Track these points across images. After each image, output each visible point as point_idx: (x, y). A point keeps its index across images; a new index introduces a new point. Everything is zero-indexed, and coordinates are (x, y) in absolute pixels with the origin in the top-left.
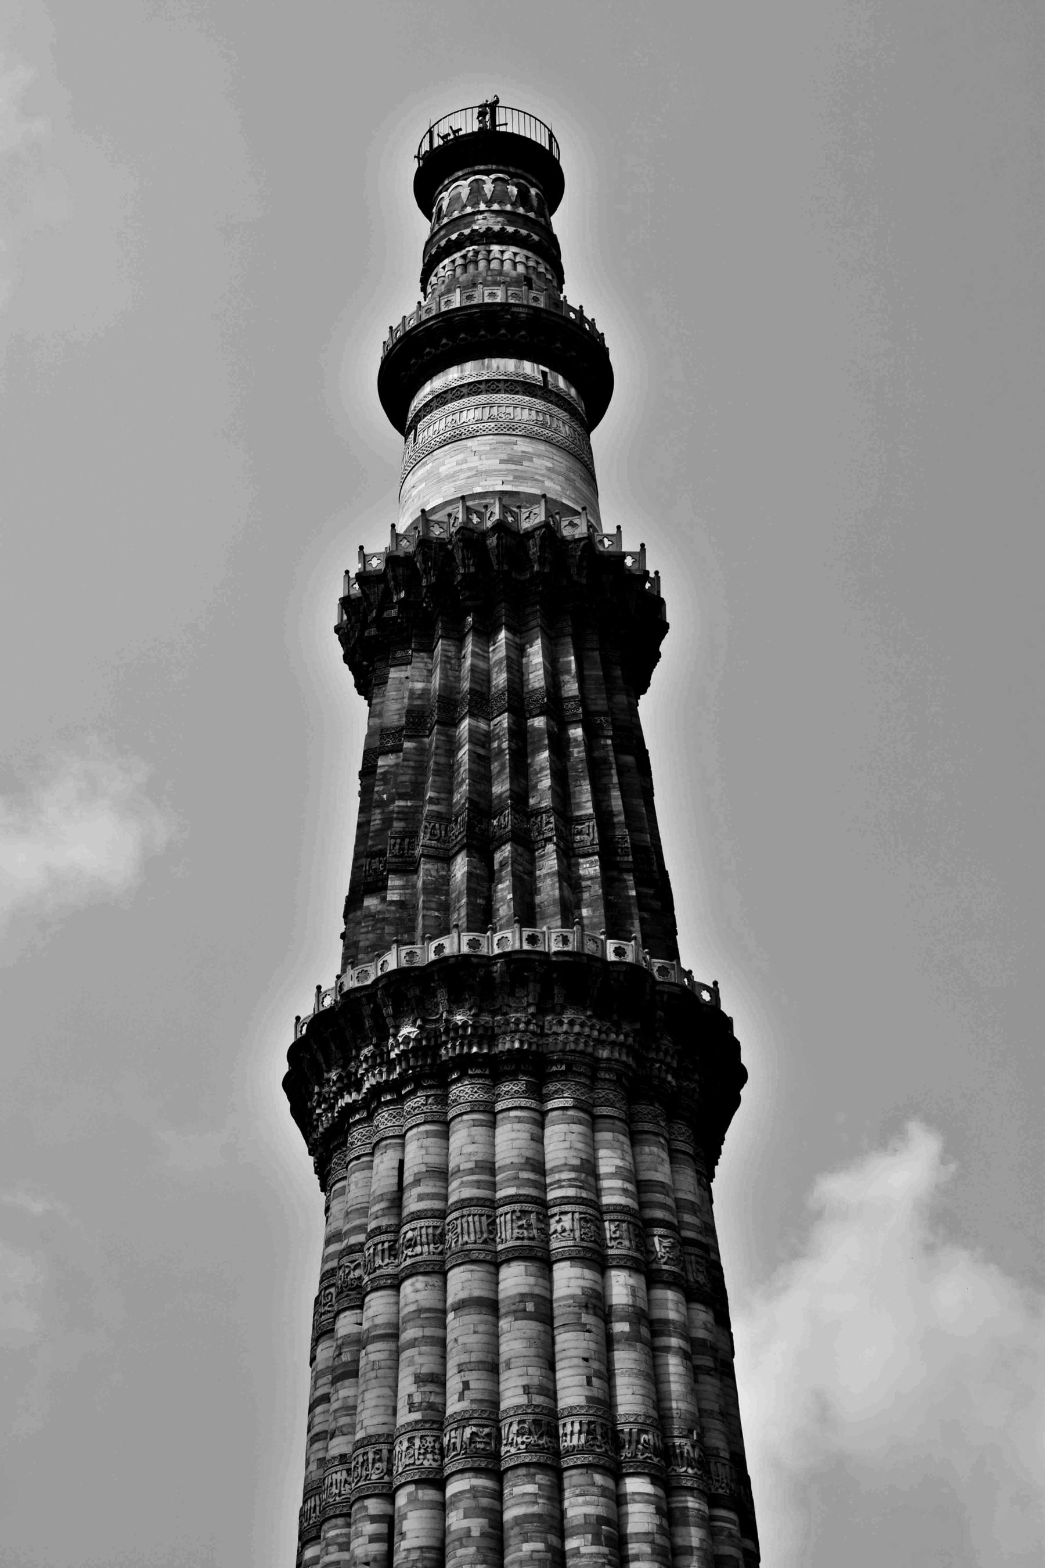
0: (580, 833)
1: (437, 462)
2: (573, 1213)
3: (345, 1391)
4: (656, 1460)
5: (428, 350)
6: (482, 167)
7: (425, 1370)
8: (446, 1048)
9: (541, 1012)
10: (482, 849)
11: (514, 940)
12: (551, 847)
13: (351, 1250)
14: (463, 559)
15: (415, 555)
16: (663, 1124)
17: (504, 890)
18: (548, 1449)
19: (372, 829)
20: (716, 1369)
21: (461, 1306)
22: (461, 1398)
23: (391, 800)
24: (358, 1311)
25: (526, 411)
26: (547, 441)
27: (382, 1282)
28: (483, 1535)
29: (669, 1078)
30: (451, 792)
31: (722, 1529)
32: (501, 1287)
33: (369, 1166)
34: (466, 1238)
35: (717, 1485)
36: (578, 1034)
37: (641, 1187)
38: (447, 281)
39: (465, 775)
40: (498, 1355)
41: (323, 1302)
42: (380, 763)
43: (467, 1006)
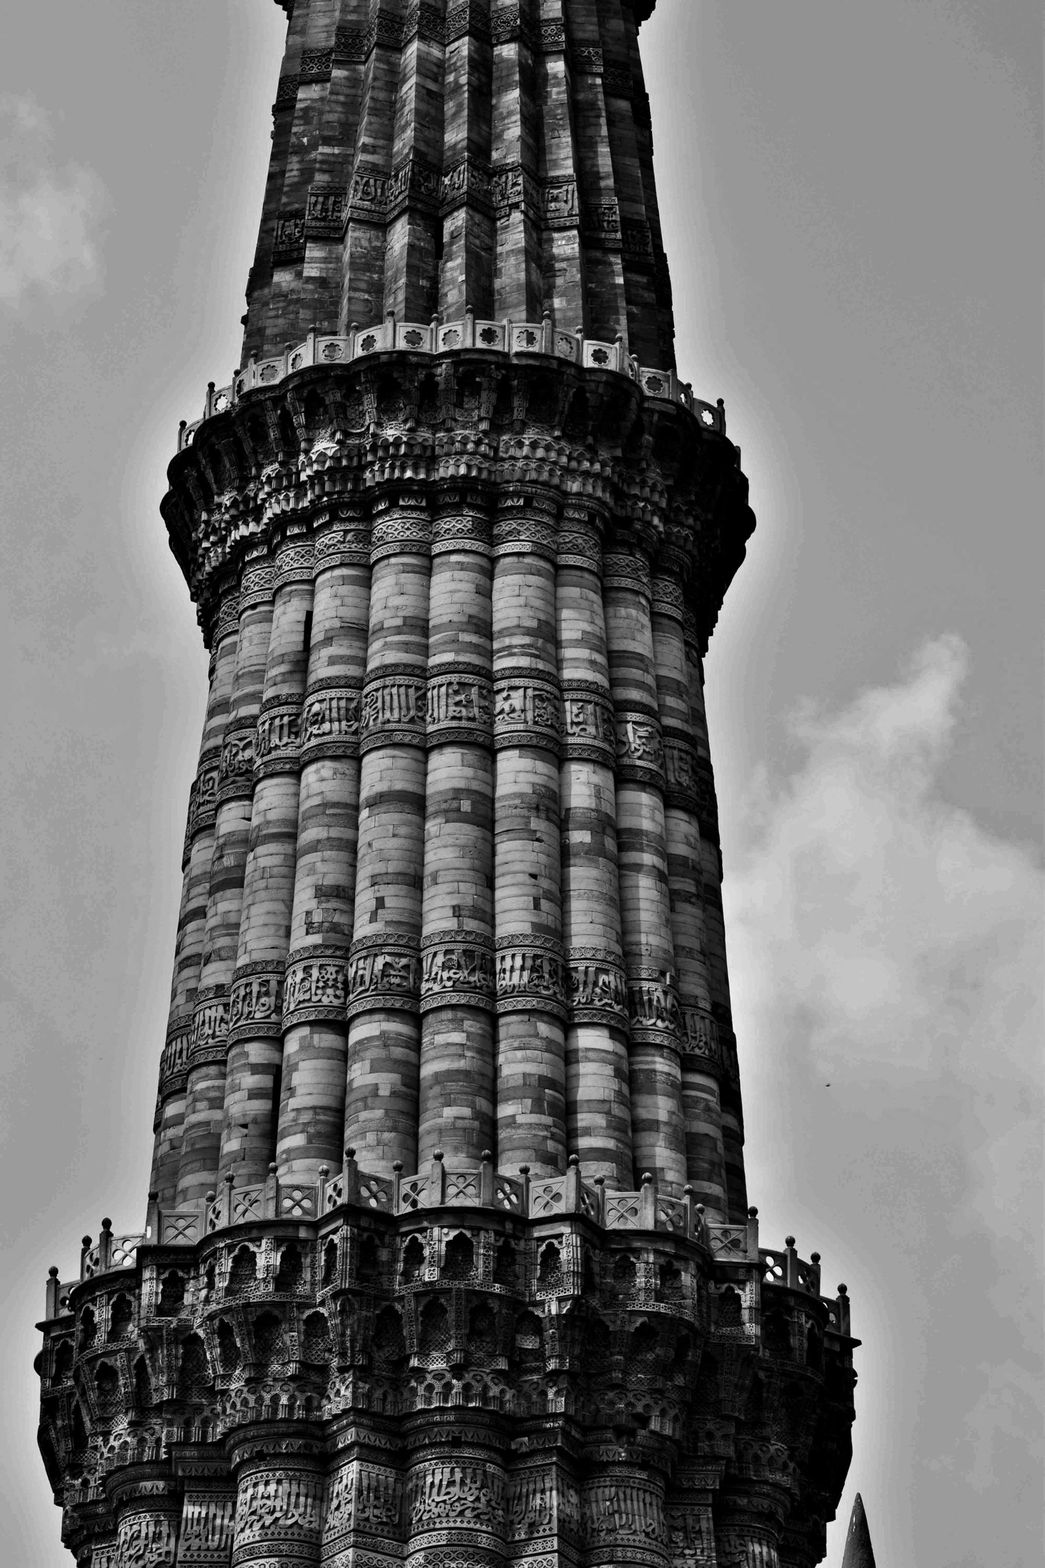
0: (555, 199)
2: (526, 688)
3: (226, 904)
4: (617, 1008)
7: (329, 881)
8: (372, 471)
9: (497, 428)
10: (428, 213)
11: (464, 335)
12: (517, 216)
13: (241, 724)
16: (645, 580)
17: (455, 270)
18: (481, 988)
19: (287, 181)
20: (698, 896)
21: (379, 800)
22: (373, 918)
24: (247, 803)
27: (278, 768)
28: (394, 1094)
29: (656, 521)
30: (390, 138)
31: (698, 1100)
32: (430, 778)
33: (268, 618)
34: (388, 715)
35: (694, 1043)
36: (540, 460)
37: (614, 659)
39: (411, 117)
40: (423, 865)
42: (300, 95)
43: (401, 418)
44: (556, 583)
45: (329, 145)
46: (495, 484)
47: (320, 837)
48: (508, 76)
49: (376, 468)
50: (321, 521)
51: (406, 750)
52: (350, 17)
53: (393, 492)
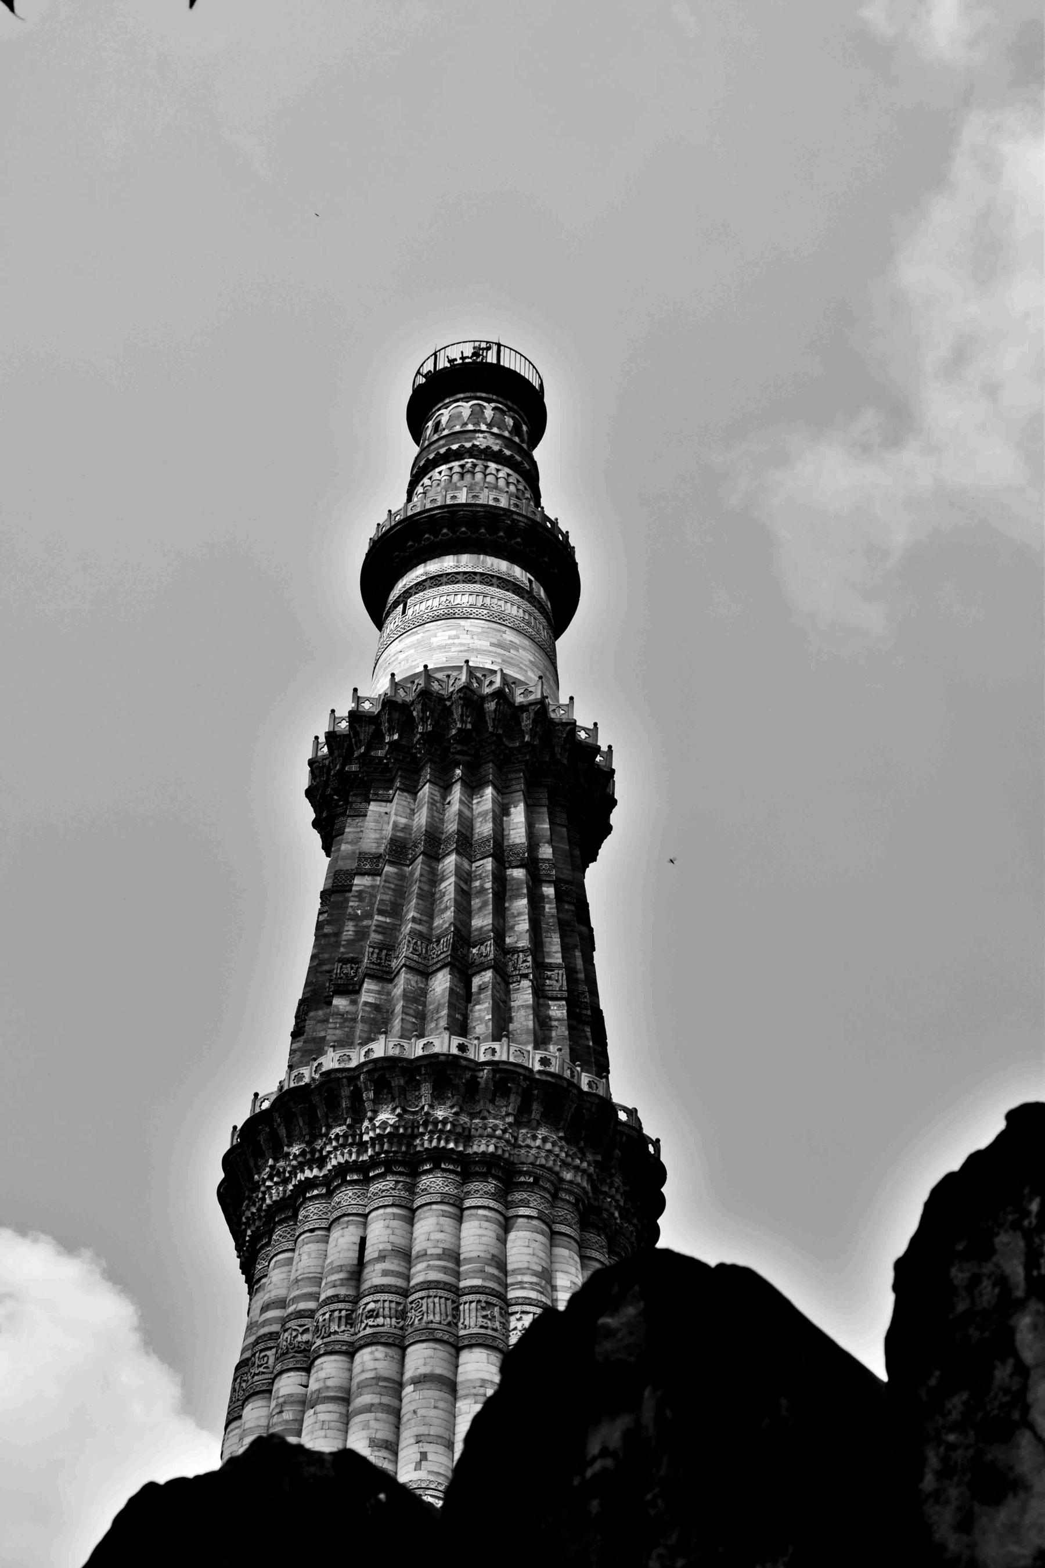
0: (549, 978)
1: (427, 634)
6: (484, 395)
7: (380, 1435)
8: (422, 1139)
9: (518, 1124)
10: (463, 971)
12: (526, 983)
13: (300, 1314)
14: (462, 715)
15: (413, 703)
19: (344, 938)
21: (417, 1381)
22: (418, 1467)
23: (369, 916)
25: (515, 607)
26: (531, 638)
27: (337, 1347)
29: (617, 1214)
30: (432, 918)
32: (460, 1370)
33: (326, 1240)
34: (431, 1317)
36: (549, 1151)
38: (443, 484)
42: (357, 881)
43: (449, 1103)
44: (552, 1245)
46: (513, 1164)
48: (517, 889)
49: (426, 1138)
50: (377, 1172)
52: (398, 834)
53: (438, 1158)
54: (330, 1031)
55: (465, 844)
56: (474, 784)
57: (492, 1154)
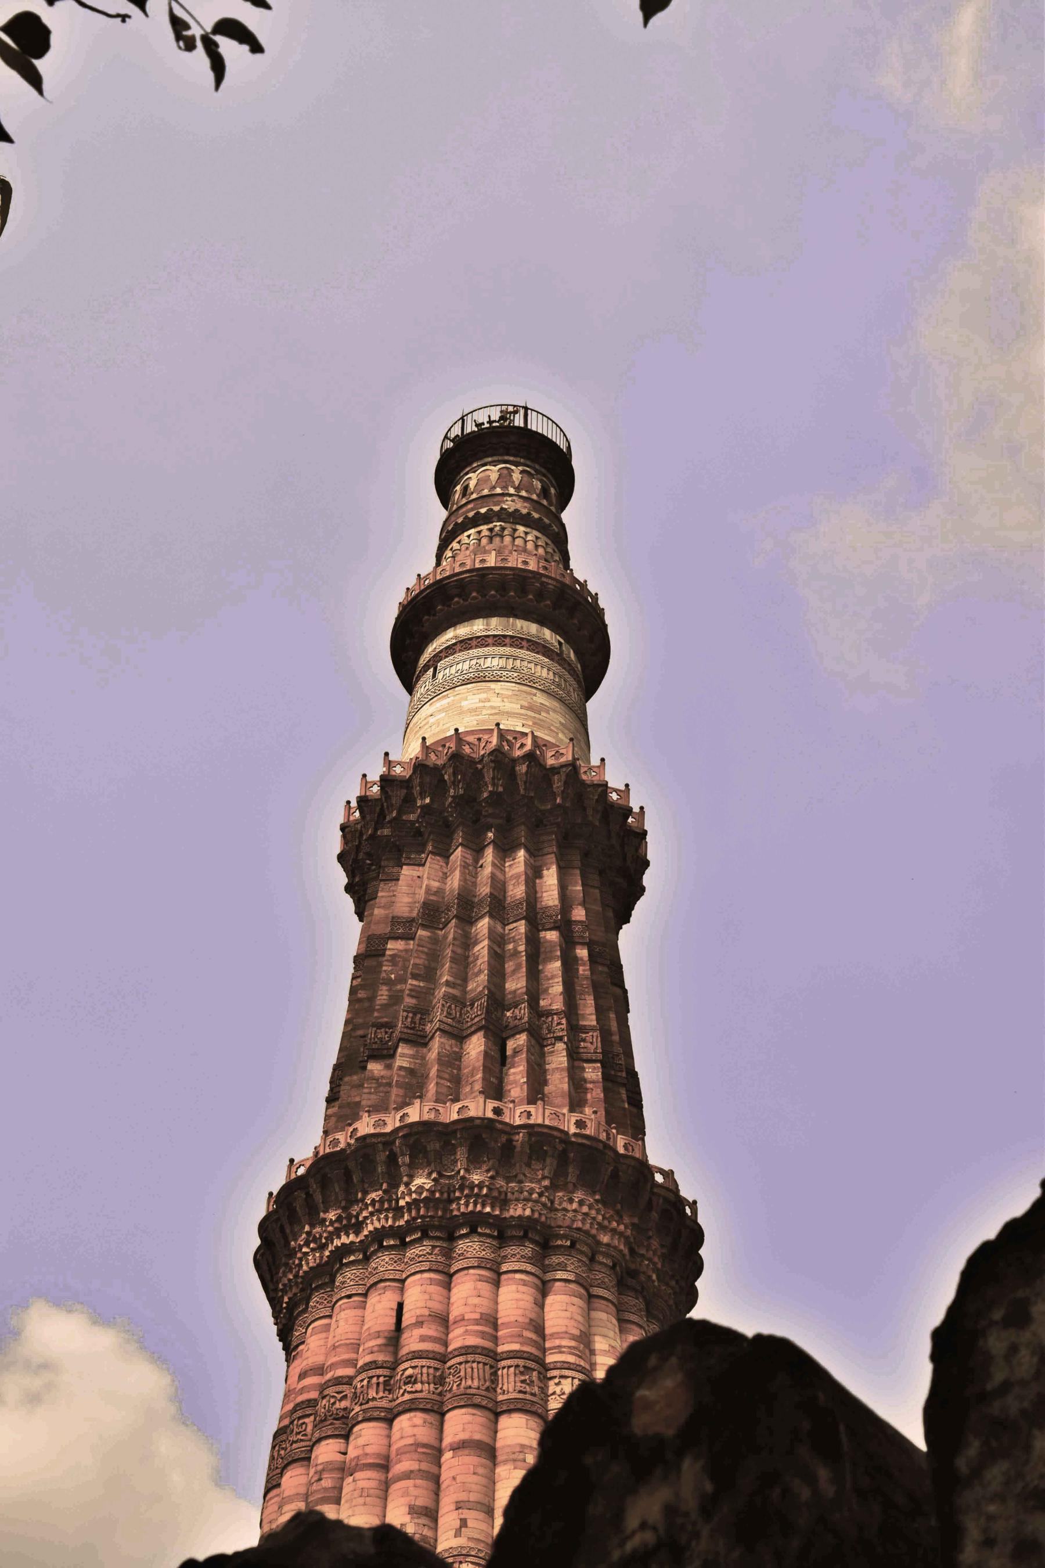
0: (584, 1040)
2: (573, 1378)
5: (456, 599)
6: (511, 458)
7: (420, 1502)
8: (458, 1204)
9: (554, 1187)
10: (498, 1035)
12: (560, 1046)
13: (338, 1381)
14: (493, 779)
19: (378, 1002)
21: (459, 1447)
22: (458, 1533)
23: (402, 980)
25: (545, 670)
26: (561, 700)
27: (376, 1414)
29: (654, 1277)
30: (465, 980)
32: (499, 1435)
33: (363, 1306)
34: (469, 1382)
38: (471, 548)
39: (485, 966)
41: (296, 1430)
42: (389, 946)
43: (485, 1168)
44: (590, 1308)
45: (416, 979)
46: (550, 1227)
47: (412, 1468)
48: (551, 952)
49: (462, 1202)
51: (483, 1410)
52: (432, 898)
53: (474, 1223)
54: (365, 1096)
55: (498, 907)
56: (507, 847)
57: (528, 1217)
